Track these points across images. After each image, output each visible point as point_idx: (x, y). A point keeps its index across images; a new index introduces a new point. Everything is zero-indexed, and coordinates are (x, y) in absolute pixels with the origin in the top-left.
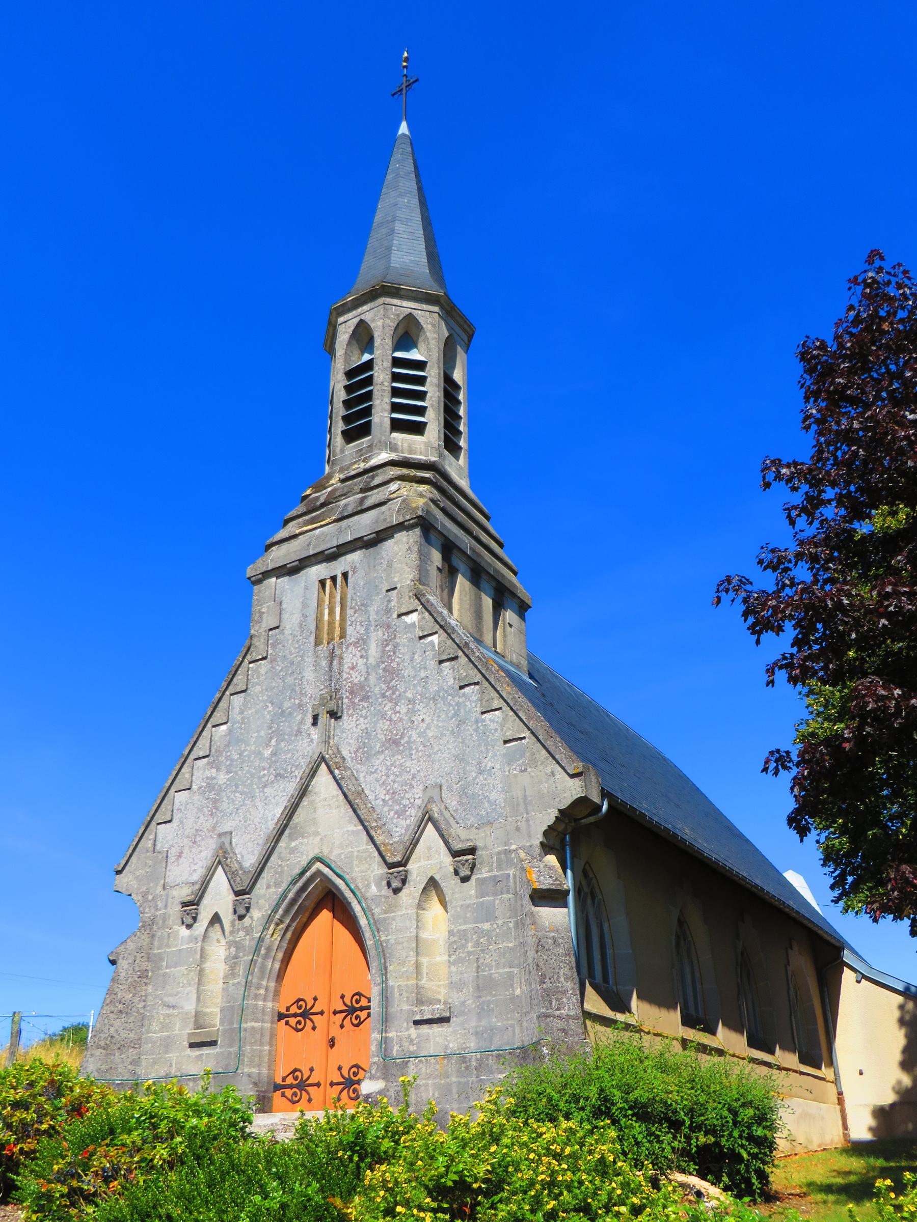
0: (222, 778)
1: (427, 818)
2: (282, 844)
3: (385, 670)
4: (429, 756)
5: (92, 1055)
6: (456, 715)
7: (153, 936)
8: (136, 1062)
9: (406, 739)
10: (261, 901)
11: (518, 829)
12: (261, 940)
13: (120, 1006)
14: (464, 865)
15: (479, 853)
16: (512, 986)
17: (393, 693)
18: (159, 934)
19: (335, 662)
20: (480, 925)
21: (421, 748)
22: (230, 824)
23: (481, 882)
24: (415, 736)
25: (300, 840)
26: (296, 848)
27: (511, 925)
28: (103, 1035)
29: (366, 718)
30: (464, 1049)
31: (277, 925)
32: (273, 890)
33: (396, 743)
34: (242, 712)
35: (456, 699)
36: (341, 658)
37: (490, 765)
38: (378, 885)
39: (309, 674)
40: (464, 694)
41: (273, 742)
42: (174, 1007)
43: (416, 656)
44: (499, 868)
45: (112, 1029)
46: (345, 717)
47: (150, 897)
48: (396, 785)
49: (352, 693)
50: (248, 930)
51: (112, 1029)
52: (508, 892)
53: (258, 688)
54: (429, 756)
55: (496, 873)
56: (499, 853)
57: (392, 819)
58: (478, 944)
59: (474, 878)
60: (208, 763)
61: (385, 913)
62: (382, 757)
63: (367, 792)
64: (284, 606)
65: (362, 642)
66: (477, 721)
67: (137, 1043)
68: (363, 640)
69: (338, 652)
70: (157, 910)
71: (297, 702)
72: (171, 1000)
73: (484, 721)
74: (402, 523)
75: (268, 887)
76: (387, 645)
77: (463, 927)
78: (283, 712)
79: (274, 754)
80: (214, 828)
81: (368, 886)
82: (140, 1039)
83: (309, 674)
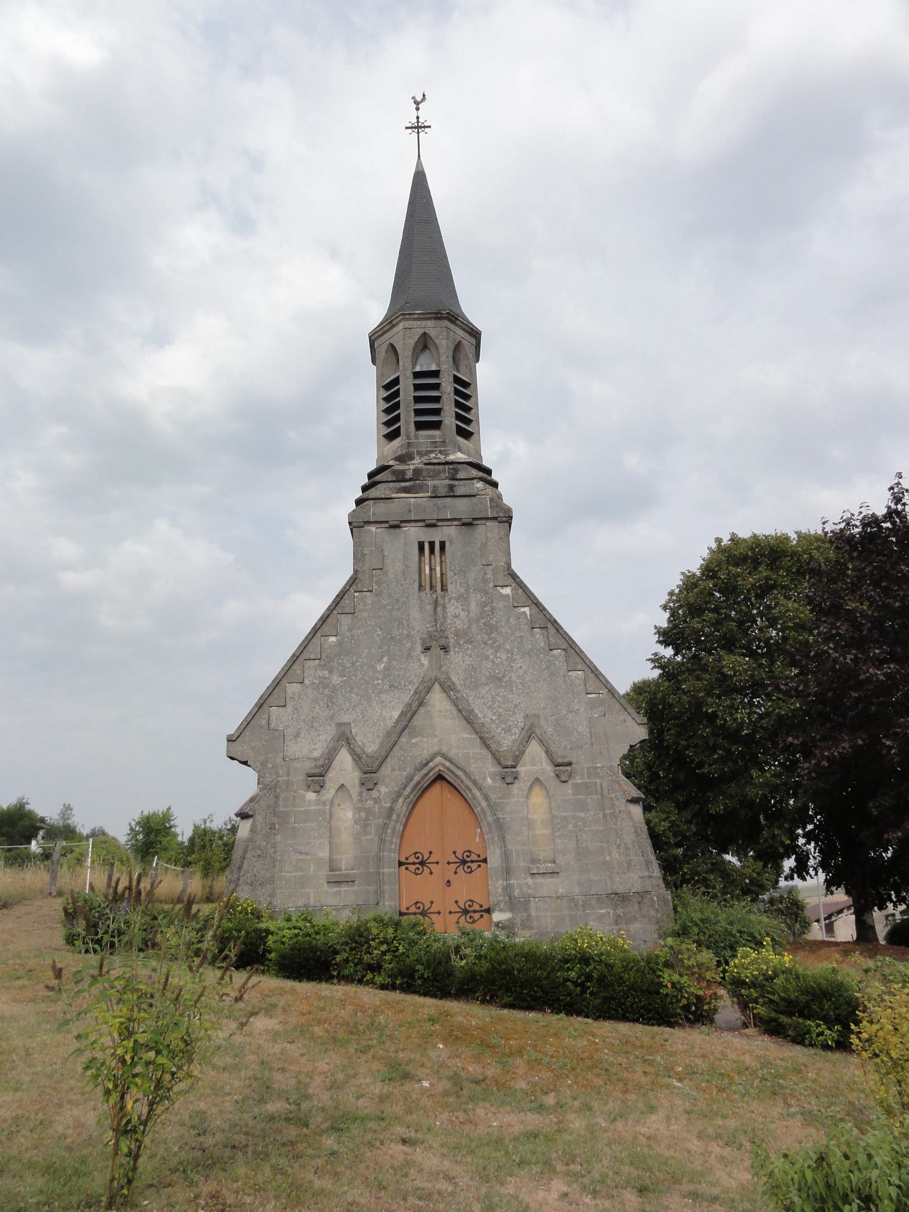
0: (336, 680)
1: (529, 735)
2: (403, 739)
3: (484, 624)
4: (528, 693)
5: (243, 890)
6: (547, 668)
7: (277, 797)
8: (272, 895)
9: (507, 678)
10: (388, 780)
11: (601, 753)
12: (391, 809)
13: (259, 852)
14: (564, 773)
15: (574, 766)
16: (603, 854)
17: (494, 643)
18: (283, 795)
19: (439, 609)
20: (577, 814)
21: (520, 687)
22: (347, 717)
23: (576, 785)
24: (514, 678)
25: (420, 738)
26: (416, 744)
27: (600, 816)
28: (249, 875)
29: (471, 656)
30: (570, 893)
31: (405, 799)
32: (397, 773)
33: (500, 680)
34: (351, 630)
35: (547, 657)
36: (444, 607)
37: (576, 707)
38: (493, 778)
39: (415, 613)
40: (553, 655)
41: (385, 659)
42: (306, 854)
43: (511, 620)
44: (589, 777)
45: (255, 870)
46: (452, 653)
47: (270, 766)
48: (501, 710)
49: (457, 635)
50: (377, 801)
51: (255, 870)
52: (597, 794)
53: (365, 614)
54: (528, 693)
55: (586, 780)
56: (588, 768)
57: (500, 733)
58: (576, 826)
59: (570, 782)
60: (319, 665)
61: (500, 799)
62: (487, 688)
63: (477, 711)
64: (386, 553)
65: (463, 599)
66: (565, 676)
67: (271, 880)
68: (464, 598)
69: (440, 601)
70: (278, 776)
71: (405, 632)
72: (303, 848)
73: (570, 676)
74: (497, 518)
75: (393, 770)
76: (485, 606)
77: (564, 814)
78: (392, 638)
79: (387, 668)
80: (332, 717)
81: (485, 779)
82: (273, 877)
83: (415, 613)
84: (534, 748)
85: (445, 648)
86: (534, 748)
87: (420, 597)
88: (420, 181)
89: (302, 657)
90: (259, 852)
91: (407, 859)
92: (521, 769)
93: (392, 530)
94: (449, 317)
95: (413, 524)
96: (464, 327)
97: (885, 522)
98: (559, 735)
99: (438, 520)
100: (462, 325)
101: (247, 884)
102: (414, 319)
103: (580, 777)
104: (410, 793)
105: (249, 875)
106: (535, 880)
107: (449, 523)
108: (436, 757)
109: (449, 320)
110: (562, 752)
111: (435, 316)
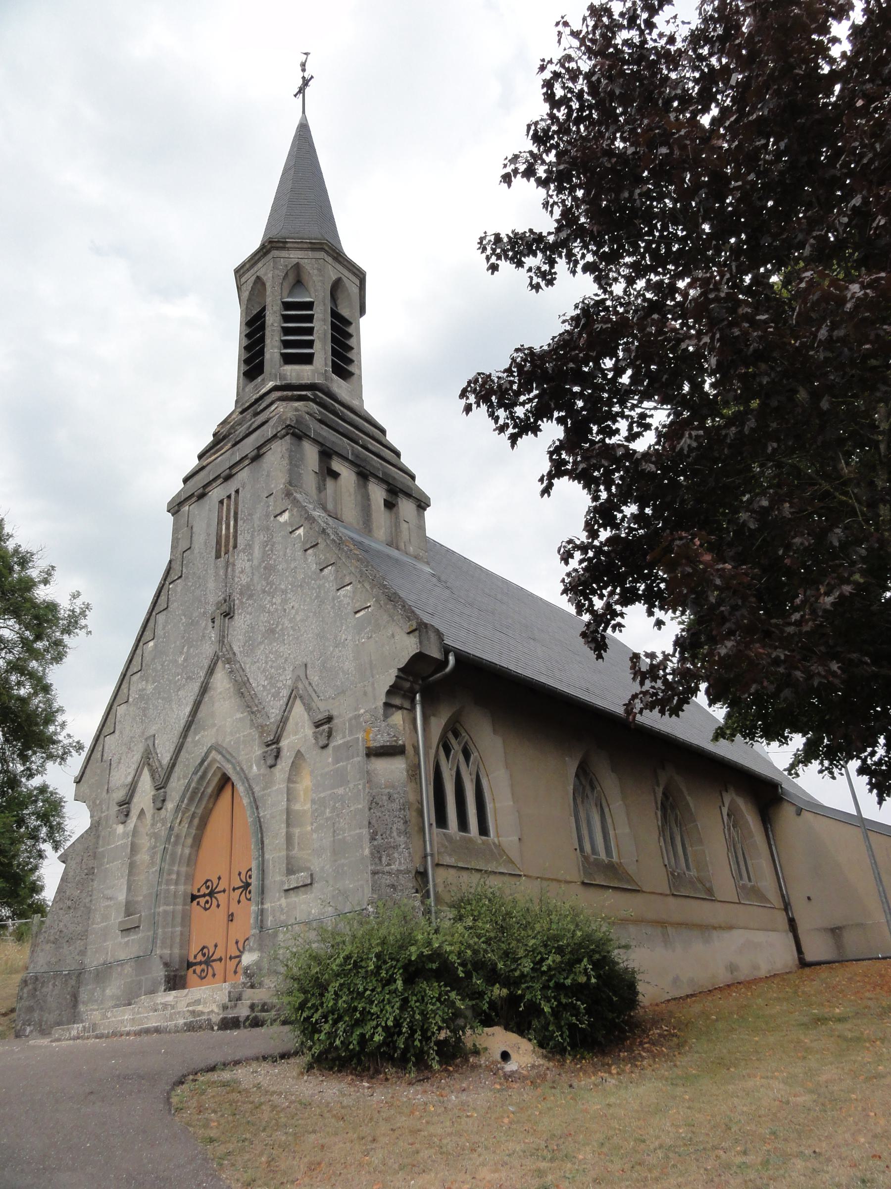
0: (150, 688)
1: (292, 697)
2: (189, 739)
3: (265, 568)
4: (297, 638)
5: (42, 950)
6: (317, 597)
7: (98, 837)
8: (83, 953)
9: (280, 627)
10: (174, 794)
11: (365, 694)
12: (171, 828)
13: (69, 903)
14: (321, 734)
15: (335, 721)
16: (362, 847)
17: (271, 587)
18: (103, 833)
19: (230, 570)
20: (335, 791)
21: (291, 632)
22: (154, 728)
23: (337, 749)
24: (287, 623)
25: (202, 733)
26: (199, 741)
27: (360, 787)
28: (52, 931)
29: (251, 614)
30: (323, 914)
31: (183, 814)
32: (182, 781)
33: (272, 631)
34: (164, 629)
35: (318, 582)
36: (234, 565)
37: (344, 637)
38: (258, 766)
39: (211, 585)
40: (323, 577)
41: (185, 650)
42: (111, 899)
43: (288, 551)
44: (351, 733)
45: (61, 925)
46: (236, 617)
47: (98, 802)
48: (273, 670)
49: (241, 594)
50: (163, 821)
51: (61, 925)
52: (358, 756)
53: (175, 604)
54: (297, 638)
55: (348, 738)
56: (351, 719)
57: (270, 701)
58: (334, 809)
59: (331, 745)
60: (141, 677)
61: (264, 790)
62: (262, 647)
63: (251, 681)
64: (194, 529)
65: (249, 546)
66: (333, 599)
67: (84, 935)
68: (249, 545)
69: (231, 560)
70: (102, 812)
71: (202, 610)
72: (109, 892)
73: (339, 597)
74: (276, 435)
75: (179, 780)
76: (267, 545)
77: (322, 795)
78: (193, 621)
79: (185, 660)
80: (143, 733)
81: (251, 767)
82: (87, 931)
83: (211, 585)
84: (298, 708)
85: (228, 614)
86: (298, 708)
87: (215, 564)
88: (303, 134)
89: (129, 674)
90: (69, 903)
91: (199, 890)
92: (284, 743)
93: (201, 501)
94: (274, 245)
95: (214, 485)
96: (299, 246)
97: (875, 149)
98: (324, 683)
99: (231, 468)
100: (296, 245)
101: (48, 942)
102: (248, 270)
103: (341, 735)
104: (188, 805)
105: (52, 931)
106: (289, 900)
107: (241, 466)
108: (211, 752)
109: (277, 248)
110: (323, 708)
111: (261, 253)
